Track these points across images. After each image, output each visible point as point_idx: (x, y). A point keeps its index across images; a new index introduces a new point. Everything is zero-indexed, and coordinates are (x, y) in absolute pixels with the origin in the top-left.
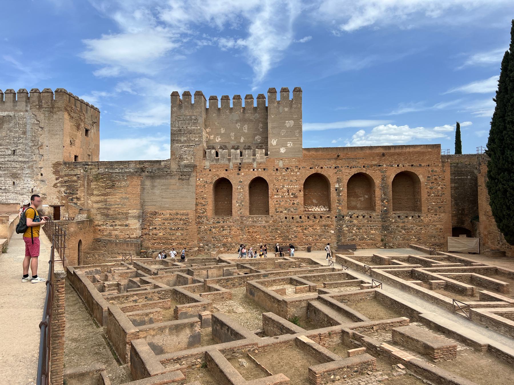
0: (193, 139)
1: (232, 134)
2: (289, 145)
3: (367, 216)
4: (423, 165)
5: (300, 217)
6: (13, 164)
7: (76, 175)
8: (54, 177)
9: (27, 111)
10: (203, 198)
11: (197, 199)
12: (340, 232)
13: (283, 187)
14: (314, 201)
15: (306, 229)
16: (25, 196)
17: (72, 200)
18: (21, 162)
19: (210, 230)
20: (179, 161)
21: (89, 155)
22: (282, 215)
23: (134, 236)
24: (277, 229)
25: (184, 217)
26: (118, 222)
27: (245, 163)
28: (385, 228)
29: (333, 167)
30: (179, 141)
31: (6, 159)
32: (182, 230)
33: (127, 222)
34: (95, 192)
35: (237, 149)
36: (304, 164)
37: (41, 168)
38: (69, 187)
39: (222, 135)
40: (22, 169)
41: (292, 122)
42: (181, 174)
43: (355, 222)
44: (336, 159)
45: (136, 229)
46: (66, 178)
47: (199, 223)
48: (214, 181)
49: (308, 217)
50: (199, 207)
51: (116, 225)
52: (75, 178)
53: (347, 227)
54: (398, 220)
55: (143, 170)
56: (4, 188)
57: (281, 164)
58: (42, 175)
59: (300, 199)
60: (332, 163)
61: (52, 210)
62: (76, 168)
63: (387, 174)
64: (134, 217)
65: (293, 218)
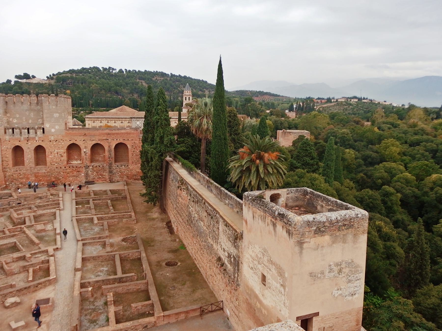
1: (24, 118)
2: (56, 127)
3: (101, 166)
4: (129, 139)
5: (65, 167)
10: (6, 157)
11: (2, 158)
12: (87, 175)
13: (55, 151)
14: (76, 157)
15: (68, 173)
19: (12, 175)
22: (54, 166)
24: (52, 174)
27: (31, 138)
28: (111, 172)
29: (82, 140)
35: (25, 129)
36: (67, 138)
39: (17, 119)
41: (58, 115)
43: (95, 169)
44: (83, 136)
48: (12, 148)
49: (69, 167)
50: (4, 163)
53: (91, 172)
54: (117, 168)
57: (52, 138)
59: (65, 157)
60: (82, 138)
63: (111, 144)
65: (61, 168)
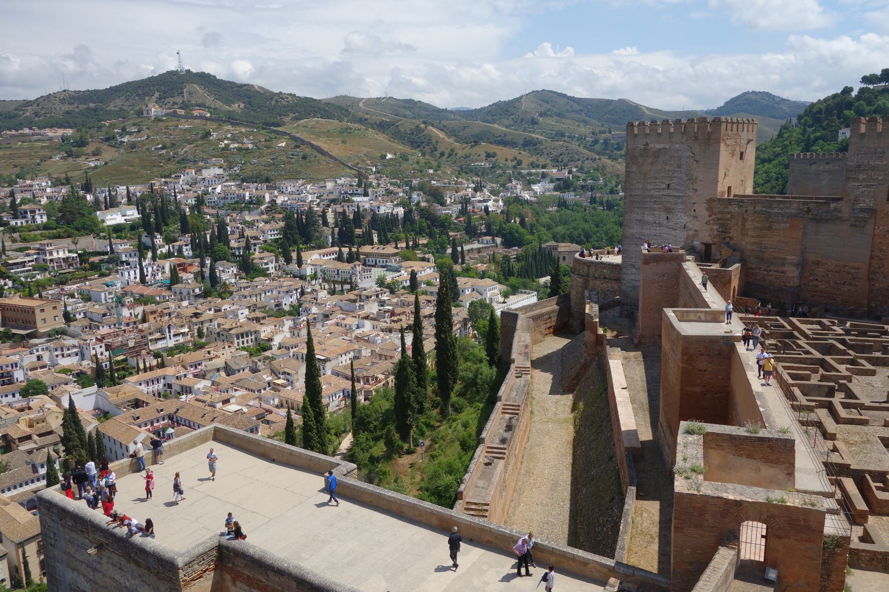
0: (875, 177)
6: (668, 198)
7: (729, 213)
8: (707, 213)
9: (682, 143)
10: (881, 250)
11: (872, 251)
16: (677, 231)
17: (724, 239)
18: (674, 196)
20: (853, 204)
21: (742, 181)
23: (791, 284)
25: (853, 271)
26: (772, 268)
30: (856, 180)
31: (661, 193)
32: (850, 284)
33: (784, 269)
34: (750, 233)
37: (694, 203)
38: (722, 225)
40: (676, 204)
42: (853, 219)
45: (793, 277)
46: (719, 216)
47: (873, 279)
51: (771, 270)
52: (729, 216)
55: (808, 211)
56: (658, 222)
58: (695, 211)
61: (703, 247)
62: (731, 205)
64: (792, 264)
